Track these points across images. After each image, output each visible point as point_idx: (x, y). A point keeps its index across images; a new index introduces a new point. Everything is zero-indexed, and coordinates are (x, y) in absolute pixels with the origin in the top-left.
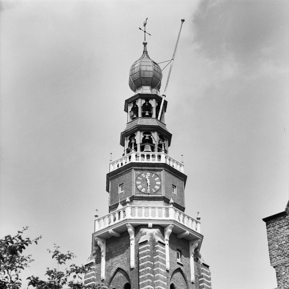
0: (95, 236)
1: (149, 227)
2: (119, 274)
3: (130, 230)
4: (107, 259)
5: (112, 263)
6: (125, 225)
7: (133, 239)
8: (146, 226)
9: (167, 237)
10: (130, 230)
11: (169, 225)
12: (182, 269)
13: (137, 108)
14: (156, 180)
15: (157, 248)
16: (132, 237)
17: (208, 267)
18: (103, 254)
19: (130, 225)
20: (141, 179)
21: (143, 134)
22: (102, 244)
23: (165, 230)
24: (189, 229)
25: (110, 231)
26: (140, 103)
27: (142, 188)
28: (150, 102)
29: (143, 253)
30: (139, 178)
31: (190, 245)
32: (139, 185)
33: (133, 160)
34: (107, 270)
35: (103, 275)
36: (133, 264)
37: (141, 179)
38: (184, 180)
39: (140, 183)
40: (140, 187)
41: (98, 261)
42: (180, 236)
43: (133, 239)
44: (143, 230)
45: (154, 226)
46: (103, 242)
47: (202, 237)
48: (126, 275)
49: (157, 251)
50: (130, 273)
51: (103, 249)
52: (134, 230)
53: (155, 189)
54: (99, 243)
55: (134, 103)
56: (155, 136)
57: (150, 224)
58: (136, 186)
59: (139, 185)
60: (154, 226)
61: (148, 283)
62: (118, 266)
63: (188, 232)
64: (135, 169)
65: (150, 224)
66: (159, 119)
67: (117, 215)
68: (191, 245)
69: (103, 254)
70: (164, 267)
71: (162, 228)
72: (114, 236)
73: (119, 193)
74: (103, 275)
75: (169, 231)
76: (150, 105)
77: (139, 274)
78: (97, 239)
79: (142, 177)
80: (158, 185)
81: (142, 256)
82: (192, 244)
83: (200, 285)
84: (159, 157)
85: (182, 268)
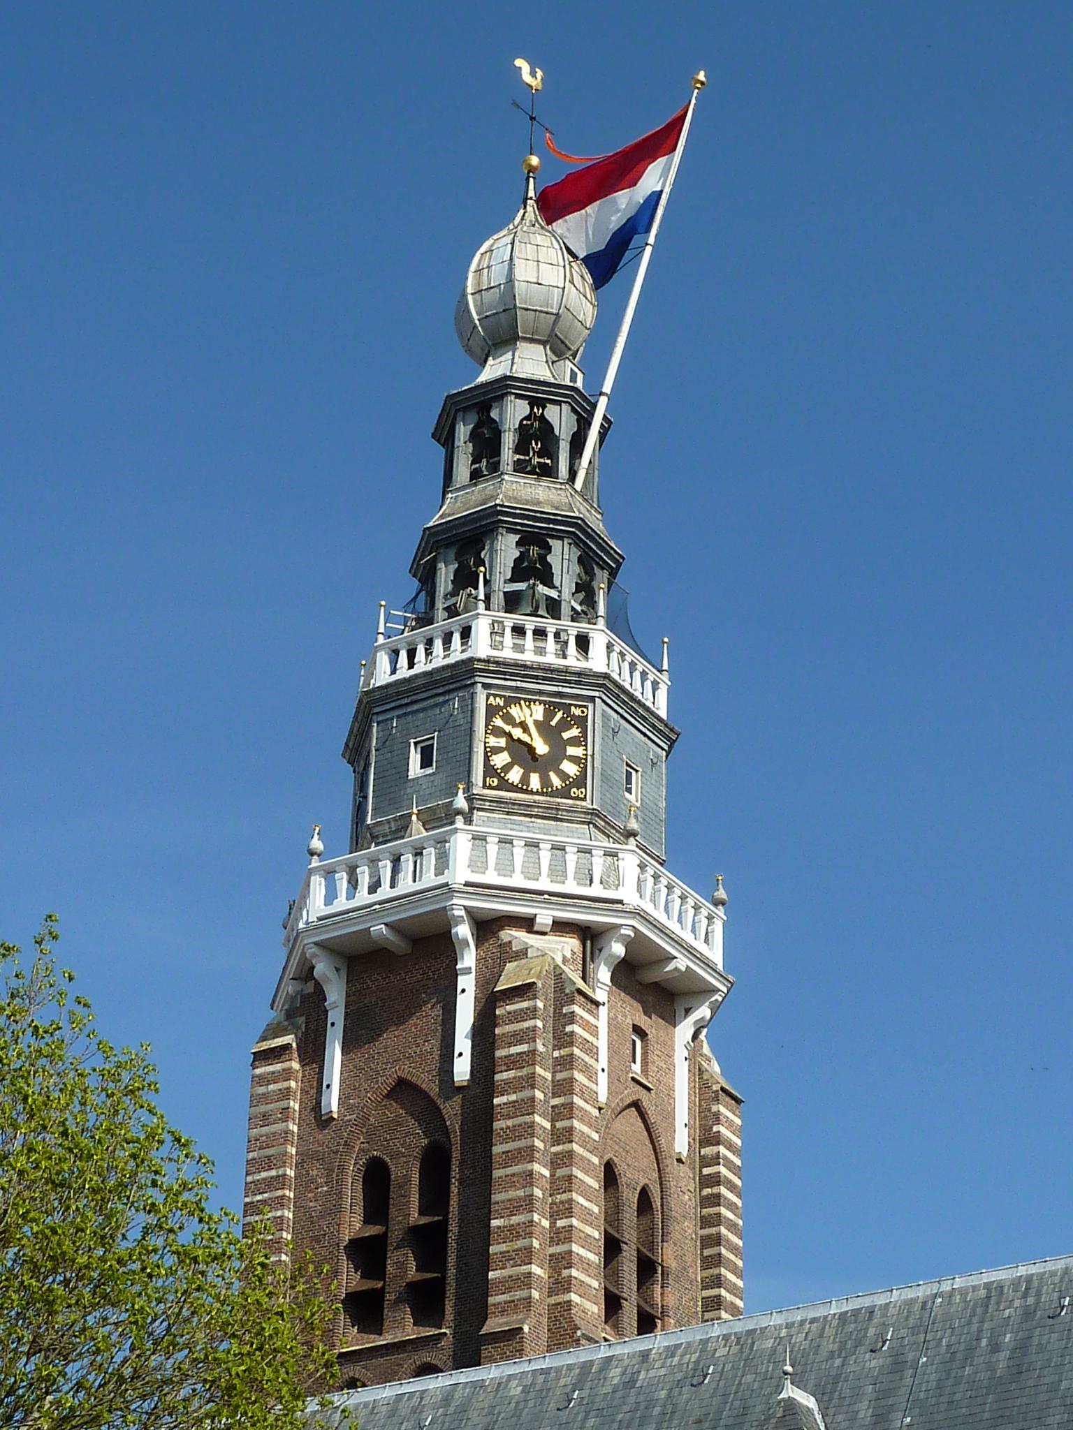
0: (305, 942)
3: (463, 931)
7: (467, 971)
8: (527, 923)
9: (604, 974)
10: (463, 931)
12: (645, 1103)
13: (497, 434)
14: (565, 738)
15: (572, 1018)
16: (468, 959)
18: (336, 1017)
19: (463, 913)
21: (518, 544)
22: (331, 974)
23: (599, 947)
24: (690, 951)
25: (379, 929)
27: (507, 768)
28: (552, 413)
29: (515, 1034)
30: (498, 722)
32: (497, 750)
33: (481, 647)
36: (462, 1069)
38: (666, 747)
40: (500, 760)
42: (651, 976)
43: (467, 971)
45: (561, 926)
46: (337, 970)
47: (729, 985)
49: (568, 1029)
51: (336, 996)
52: (475, 933)
53: (563, 776)
54: (322, 968)
56: (562, 557)
57: (544, 917)
58: (490, 752)
59: (497, 750)
60: (561, 926)
63: (682, 963)
64: (485, 686)
65: (544, 917)
66: (579, 484)
68: (683, 1012)
69: (336, 1017)
70: (592, 1097)
71: (591, 936)
72: (384, 950)
73: (411, 775)
75: (618, 949)
76: (546, 426)
78: (314, 955)
80: (575, 760)
82: (688, 1011)
83: (706, 1171)
84: (583, 643)
85: (646, 1102)
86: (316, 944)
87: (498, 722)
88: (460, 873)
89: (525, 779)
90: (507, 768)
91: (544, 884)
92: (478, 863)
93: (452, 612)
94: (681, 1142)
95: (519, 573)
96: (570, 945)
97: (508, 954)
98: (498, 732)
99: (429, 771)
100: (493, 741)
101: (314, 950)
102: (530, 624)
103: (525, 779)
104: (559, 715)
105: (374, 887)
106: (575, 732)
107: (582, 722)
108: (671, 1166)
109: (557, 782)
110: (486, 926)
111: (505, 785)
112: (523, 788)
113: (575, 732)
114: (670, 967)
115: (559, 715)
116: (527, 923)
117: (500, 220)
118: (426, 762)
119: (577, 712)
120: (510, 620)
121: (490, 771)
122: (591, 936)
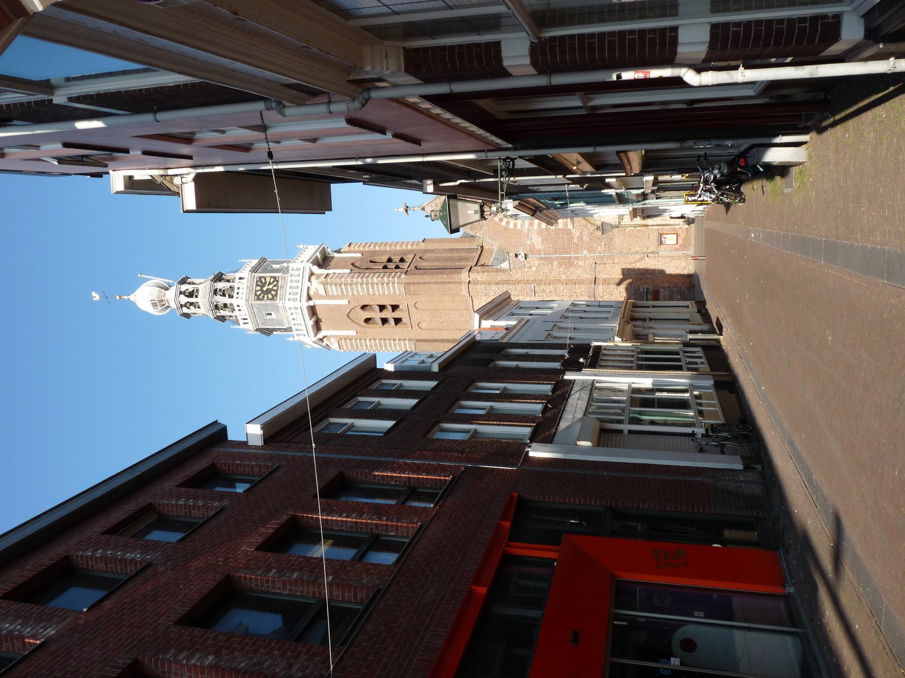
20: (262, 295)
26: (184, 299)
27: (272, 295)
30: (261, 297)
31: (329, 255)
32: (268, 297)
37: (262, 295)
39: (266, 296)
42: (320, 261)
55: (182, 306)
56: (220, 285)
59: (268, 297)
63: (318, 254)
65: (307, 284)
71: (312, 274)
79: (260, 295)
82: (329, 254)
84: (240, 278)
87: (261, 297)
88: (298, 304)
89: (274, 290)
90: (272, 295)
91: (299, 284)
92: (295, 300)
93: (233, 310)
95: (224, 295)
97: (316, 293)
98: (263, 297)
99: (273, 313)
100: (266, 298)
102: (236, 291)
103: (274, 290)
104: (259, 283)
105: (301, 325)
106: (263, 279)
107: (260, 278)
109: (275, 283)
110: (309, 298)
111: (276, 295)
112: (276, 291)
113: (263, 279)
114: (319, 256)
115: (259, 283)
117: (133, 305)
118: (270, 314)
119: (258, 279)
120: (235, 295)
121: (273, 299)
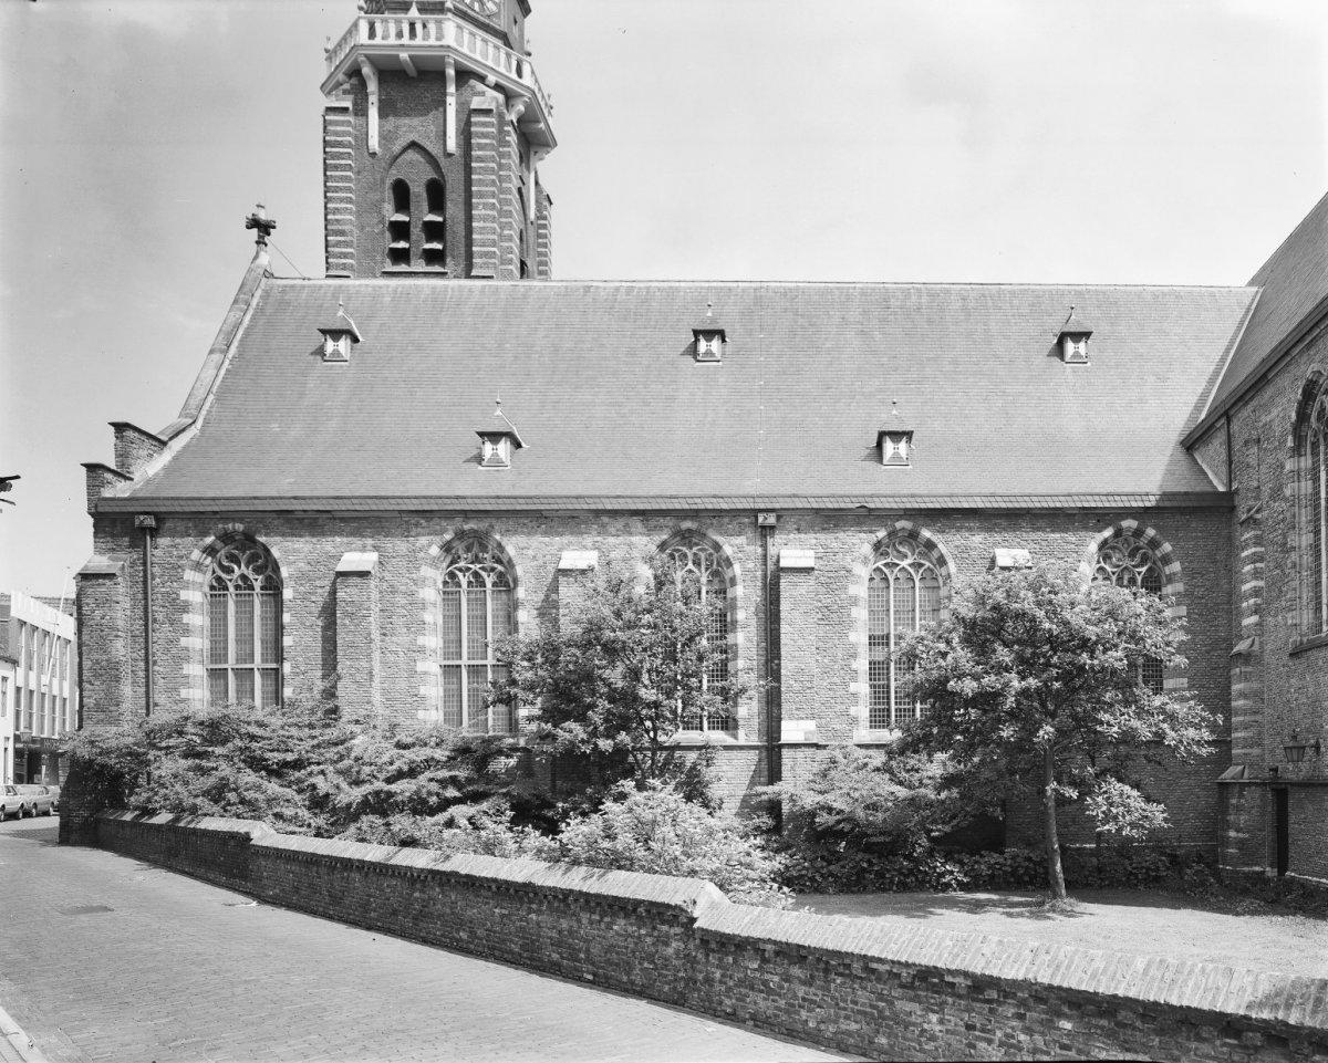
1: (487, 83)
2: (412, 155)
3: (451, 72)
4: (383, 114)
5: (397, 127)
6: (443, 57)
8: (482, 79)
10: (451, 72)
11: (523, 96)
16: (451, 89)
17: (551, 203)
18: (373, 99)
25: (404, 55)
34: (385, 138)
35: (374, 143)
41: (360, 110)
44: (480, 87)
45: (498, 87)
48: (432, 160)
50: (443, 162)
54: (366, 70)
57: (492, 79)
61: (493, 195)
62: (413, 137)
63: (542, 125)
65: (492, 79)
67: (406, 28)
69: (373, 99)
71: (509, 97)
72: (405, 71)
74: (374, 143)
77: (468, 171)
78: (362, 61)
81: (479, 138)
86: (366, 56)
94: (532, 214)
96: (501, 97)
101: (364, 59)
108: (529, 222)
116: (482, 79)
122: (509, 97)
